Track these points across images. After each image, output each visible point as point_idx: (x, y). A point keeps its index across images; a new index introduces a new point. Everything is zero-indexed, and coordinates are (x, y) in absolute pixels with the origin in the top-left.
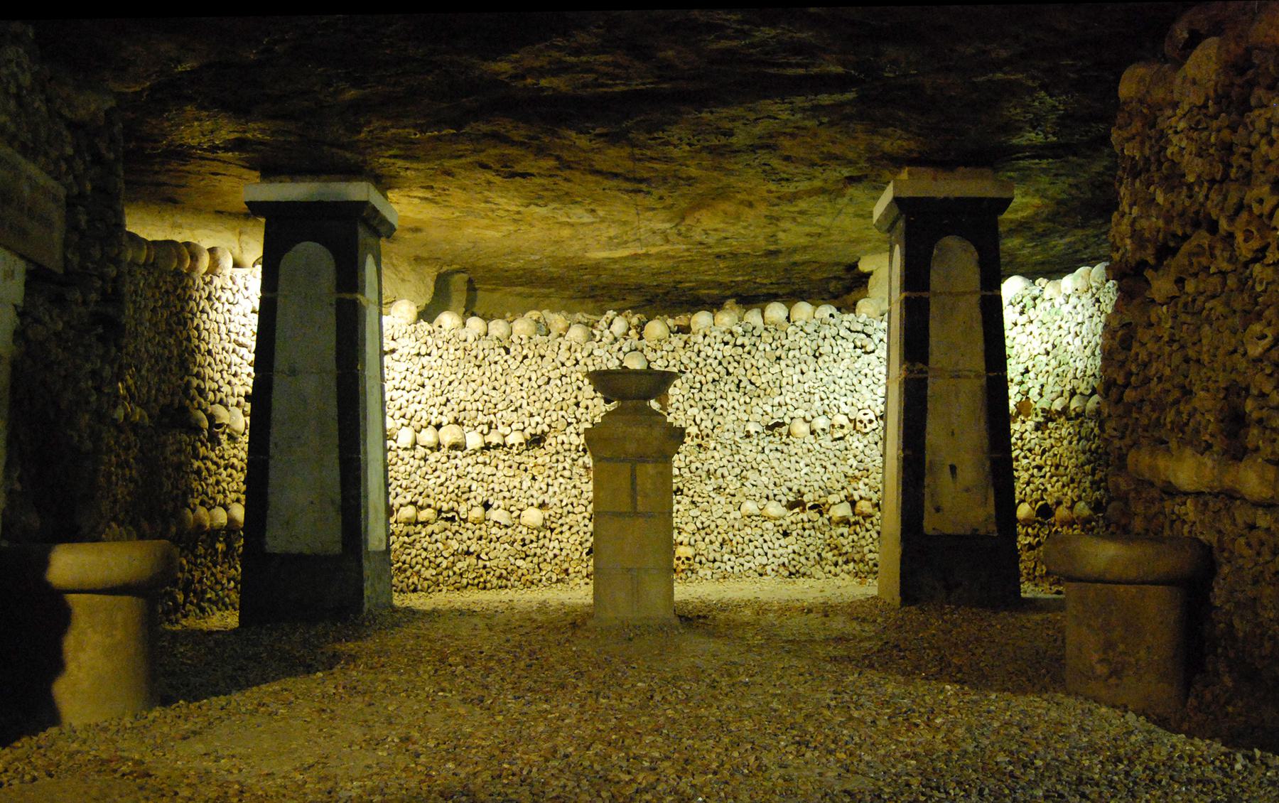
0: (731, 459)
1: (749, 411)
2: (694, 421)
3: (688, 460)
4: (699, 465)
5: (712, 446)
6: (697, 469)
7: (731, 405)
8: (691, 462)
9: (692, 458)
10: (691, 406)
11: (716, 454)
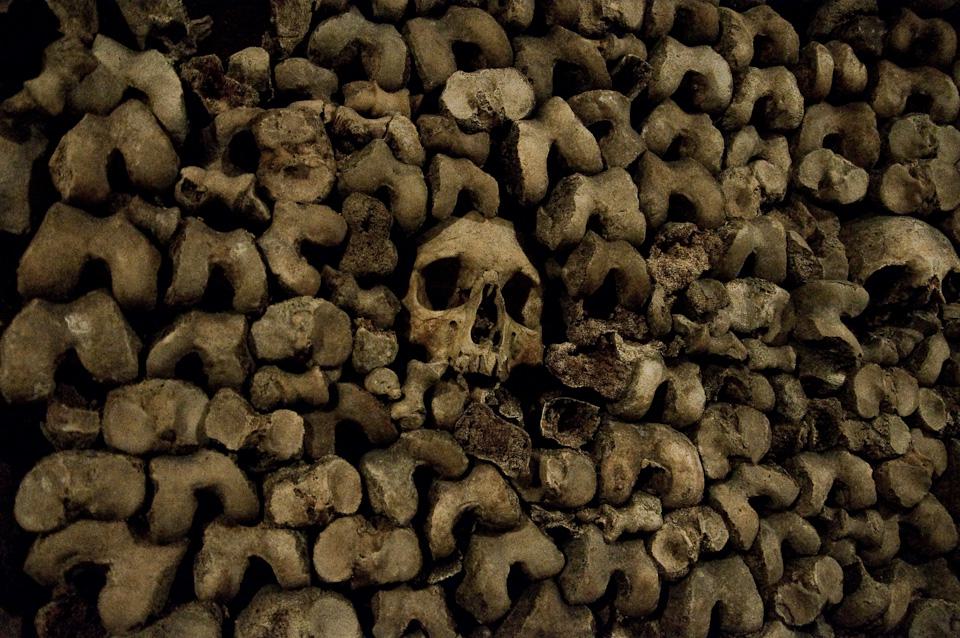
0: (779, 483)
1: (871, 142)
2: (501, 159)
3: (443, 513)
4: (534, 548)
5: (651, 374)
6: (521, 580)
7: (757, 83)
8: (472, 525)
9: (487, 489)
10: (469, 56)
11: (678, 452)
